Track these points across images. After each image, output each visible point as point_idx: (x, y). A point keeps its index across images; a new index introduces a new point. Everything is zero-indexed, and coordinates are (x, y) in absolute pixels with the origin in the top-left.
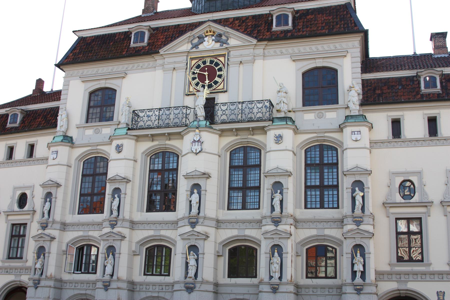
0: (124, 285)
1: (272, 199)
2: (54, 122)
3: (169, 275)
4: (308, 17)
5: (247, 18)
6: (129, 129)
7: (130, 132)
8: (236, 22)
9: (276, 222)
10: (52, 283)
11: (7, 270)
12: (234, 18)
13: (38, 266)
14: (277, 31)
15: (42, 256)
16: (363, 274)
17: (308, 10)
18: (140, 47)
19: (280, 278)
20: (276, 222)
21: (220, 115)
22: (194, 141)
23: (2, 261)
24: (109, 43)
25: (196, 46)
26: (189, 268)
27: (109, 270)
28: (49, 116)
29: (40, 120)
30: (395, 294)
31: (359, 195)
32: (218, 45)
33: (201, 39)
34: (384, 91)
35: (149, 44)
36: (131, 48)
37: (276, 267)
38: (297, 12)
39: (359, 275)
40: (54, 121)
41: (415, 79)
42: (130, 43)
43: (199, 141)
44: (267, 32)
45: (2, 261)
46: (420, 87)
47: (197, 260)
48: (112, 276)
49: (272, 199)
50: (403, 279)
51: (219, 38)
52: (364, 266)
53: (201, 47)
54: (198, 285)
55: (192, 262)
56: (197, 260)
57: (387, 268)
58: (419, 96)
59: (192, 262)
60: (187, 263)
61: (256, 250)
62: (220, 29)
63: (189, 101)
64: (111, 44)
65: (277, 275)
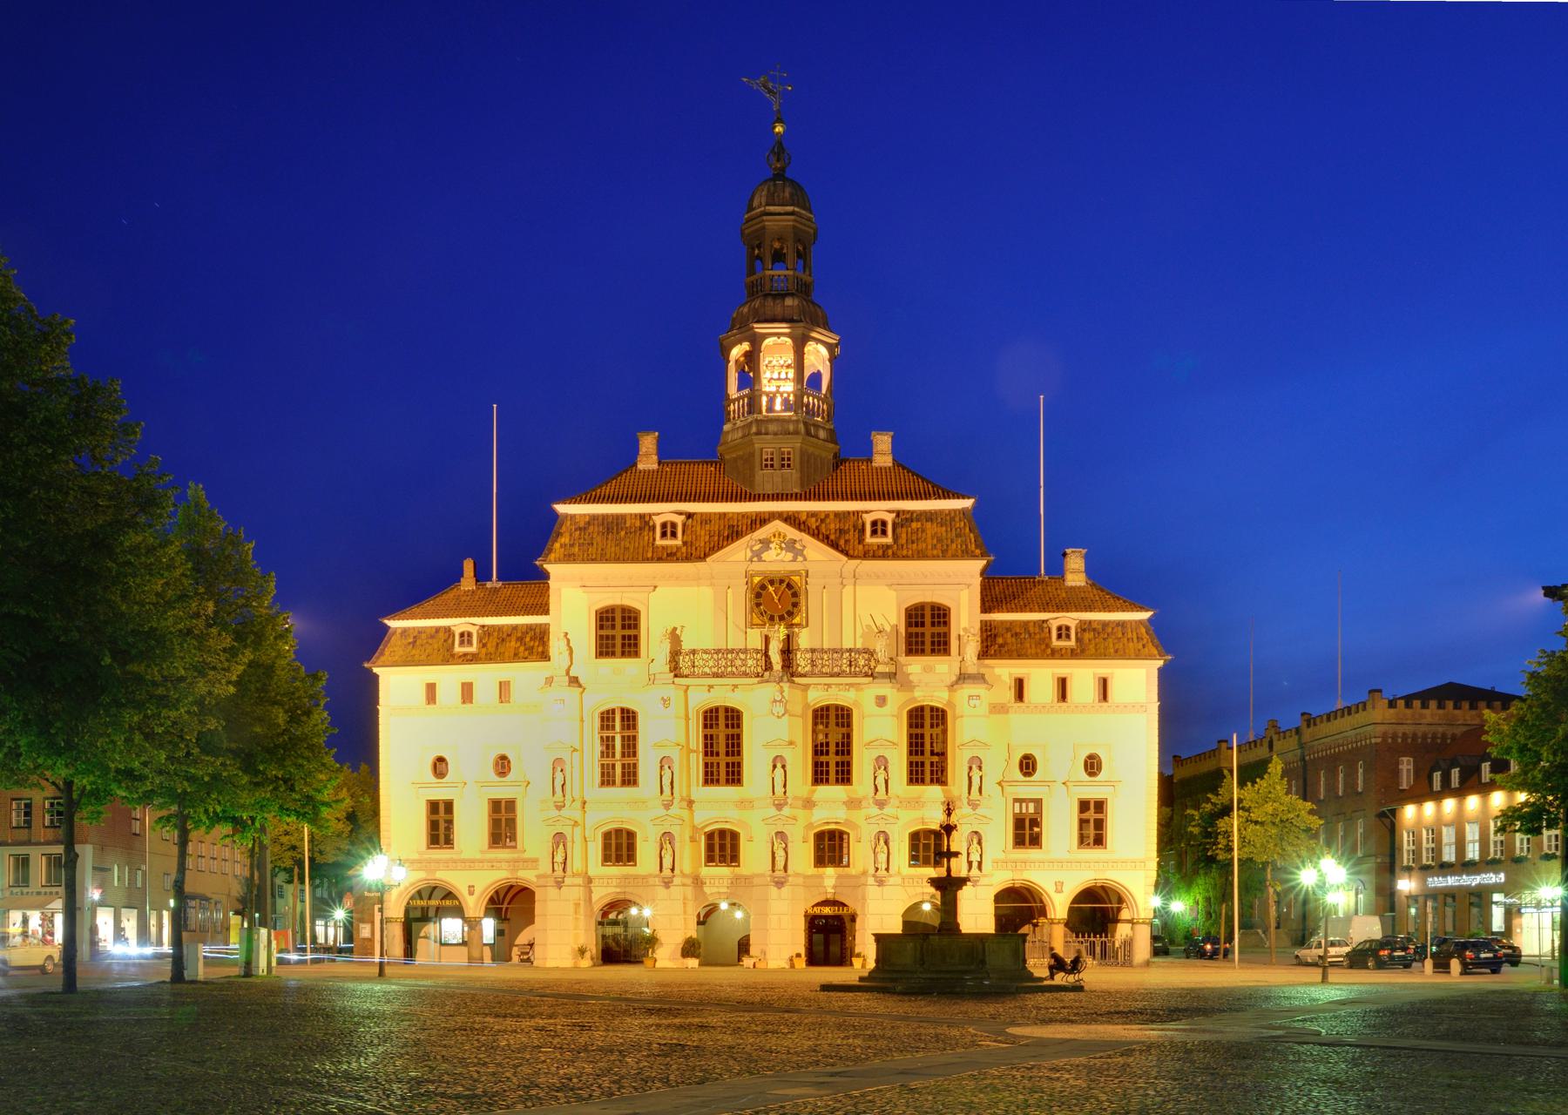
0: (689, 881)
1: (875, 778)
2: (543, 652)
3: (739, 866)
4: (914, 525)
5: (827, 515)
6: (676, 676)
7: (677, 680)
8: (813, 520)
9: (881, 804)
10: (579, 881)
11: (493, 865)
12: (808, 513)
13: (559, 858)
14: (872, 545)
15: (561, 846)
16: (980, 864)
17: (912, 512)
18: (671, 546)
19: (887, 869)
20: (881, 804)
21: (802, 661)
22: (775, 701)
23: (482, 852)
24: (618, 533)
25: (757, 555)
26: (777, 859)
27: (667, 863)
28: (528, 639)
29: (513, 643)
30: (1008, 885)
31: (976, 775)
32: (790, 556)
33: (766, 543)
34: (1009, 641)
35: (685, 543)
36: (657, 547)
37: (882, 857)
38: (898, 513)
39: (975, 865)
40: (540, 649)
41: (1045, 625)
42: (654, 539)
43: (780, 701)
44: (859, 543)
45: (482, 852)
46: (1050, 638)
47: (785, 850)
48: (673, 870)
49: (875, 778)
50: (1019, 867)
51: (790, 546)
52: (981, 856)
53: (765, 556)
54: (790, 879)
55: (780, 854)
56: (785, 850)
57: (1002, 856)
58: (1049, 651)
59: (780, 854)
60: (773, 853)
61: (848, 834)
62: (791, 533)
63: (755, 639)
64: (623, 533)
65: (884, 866)
